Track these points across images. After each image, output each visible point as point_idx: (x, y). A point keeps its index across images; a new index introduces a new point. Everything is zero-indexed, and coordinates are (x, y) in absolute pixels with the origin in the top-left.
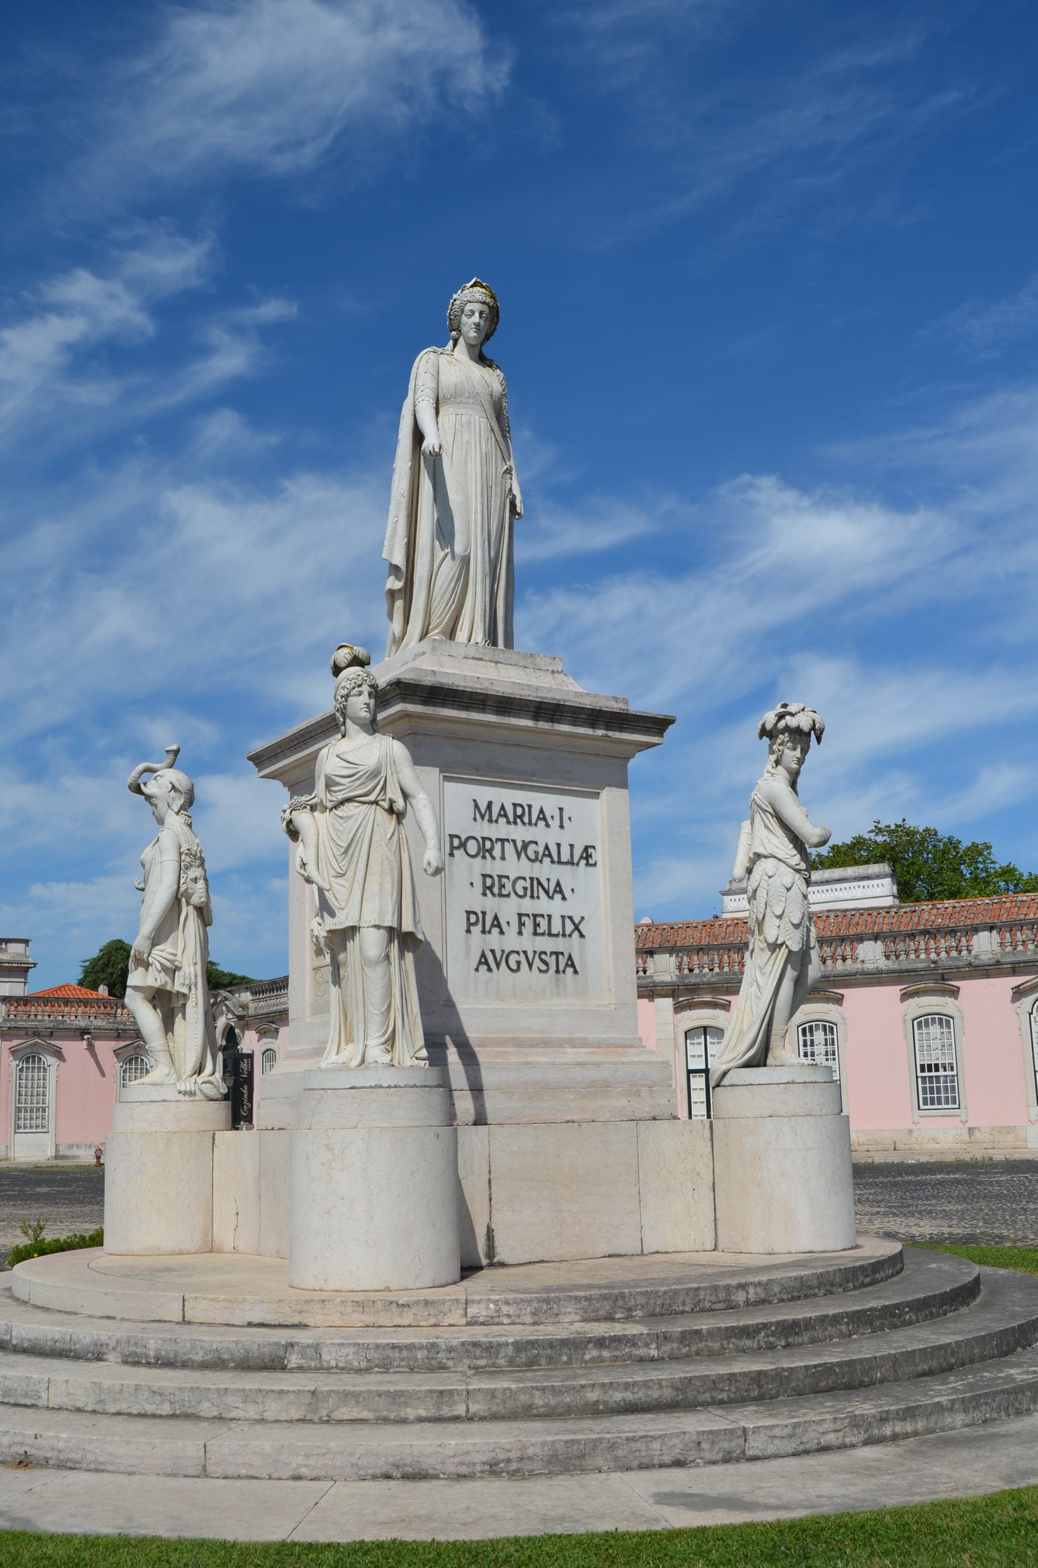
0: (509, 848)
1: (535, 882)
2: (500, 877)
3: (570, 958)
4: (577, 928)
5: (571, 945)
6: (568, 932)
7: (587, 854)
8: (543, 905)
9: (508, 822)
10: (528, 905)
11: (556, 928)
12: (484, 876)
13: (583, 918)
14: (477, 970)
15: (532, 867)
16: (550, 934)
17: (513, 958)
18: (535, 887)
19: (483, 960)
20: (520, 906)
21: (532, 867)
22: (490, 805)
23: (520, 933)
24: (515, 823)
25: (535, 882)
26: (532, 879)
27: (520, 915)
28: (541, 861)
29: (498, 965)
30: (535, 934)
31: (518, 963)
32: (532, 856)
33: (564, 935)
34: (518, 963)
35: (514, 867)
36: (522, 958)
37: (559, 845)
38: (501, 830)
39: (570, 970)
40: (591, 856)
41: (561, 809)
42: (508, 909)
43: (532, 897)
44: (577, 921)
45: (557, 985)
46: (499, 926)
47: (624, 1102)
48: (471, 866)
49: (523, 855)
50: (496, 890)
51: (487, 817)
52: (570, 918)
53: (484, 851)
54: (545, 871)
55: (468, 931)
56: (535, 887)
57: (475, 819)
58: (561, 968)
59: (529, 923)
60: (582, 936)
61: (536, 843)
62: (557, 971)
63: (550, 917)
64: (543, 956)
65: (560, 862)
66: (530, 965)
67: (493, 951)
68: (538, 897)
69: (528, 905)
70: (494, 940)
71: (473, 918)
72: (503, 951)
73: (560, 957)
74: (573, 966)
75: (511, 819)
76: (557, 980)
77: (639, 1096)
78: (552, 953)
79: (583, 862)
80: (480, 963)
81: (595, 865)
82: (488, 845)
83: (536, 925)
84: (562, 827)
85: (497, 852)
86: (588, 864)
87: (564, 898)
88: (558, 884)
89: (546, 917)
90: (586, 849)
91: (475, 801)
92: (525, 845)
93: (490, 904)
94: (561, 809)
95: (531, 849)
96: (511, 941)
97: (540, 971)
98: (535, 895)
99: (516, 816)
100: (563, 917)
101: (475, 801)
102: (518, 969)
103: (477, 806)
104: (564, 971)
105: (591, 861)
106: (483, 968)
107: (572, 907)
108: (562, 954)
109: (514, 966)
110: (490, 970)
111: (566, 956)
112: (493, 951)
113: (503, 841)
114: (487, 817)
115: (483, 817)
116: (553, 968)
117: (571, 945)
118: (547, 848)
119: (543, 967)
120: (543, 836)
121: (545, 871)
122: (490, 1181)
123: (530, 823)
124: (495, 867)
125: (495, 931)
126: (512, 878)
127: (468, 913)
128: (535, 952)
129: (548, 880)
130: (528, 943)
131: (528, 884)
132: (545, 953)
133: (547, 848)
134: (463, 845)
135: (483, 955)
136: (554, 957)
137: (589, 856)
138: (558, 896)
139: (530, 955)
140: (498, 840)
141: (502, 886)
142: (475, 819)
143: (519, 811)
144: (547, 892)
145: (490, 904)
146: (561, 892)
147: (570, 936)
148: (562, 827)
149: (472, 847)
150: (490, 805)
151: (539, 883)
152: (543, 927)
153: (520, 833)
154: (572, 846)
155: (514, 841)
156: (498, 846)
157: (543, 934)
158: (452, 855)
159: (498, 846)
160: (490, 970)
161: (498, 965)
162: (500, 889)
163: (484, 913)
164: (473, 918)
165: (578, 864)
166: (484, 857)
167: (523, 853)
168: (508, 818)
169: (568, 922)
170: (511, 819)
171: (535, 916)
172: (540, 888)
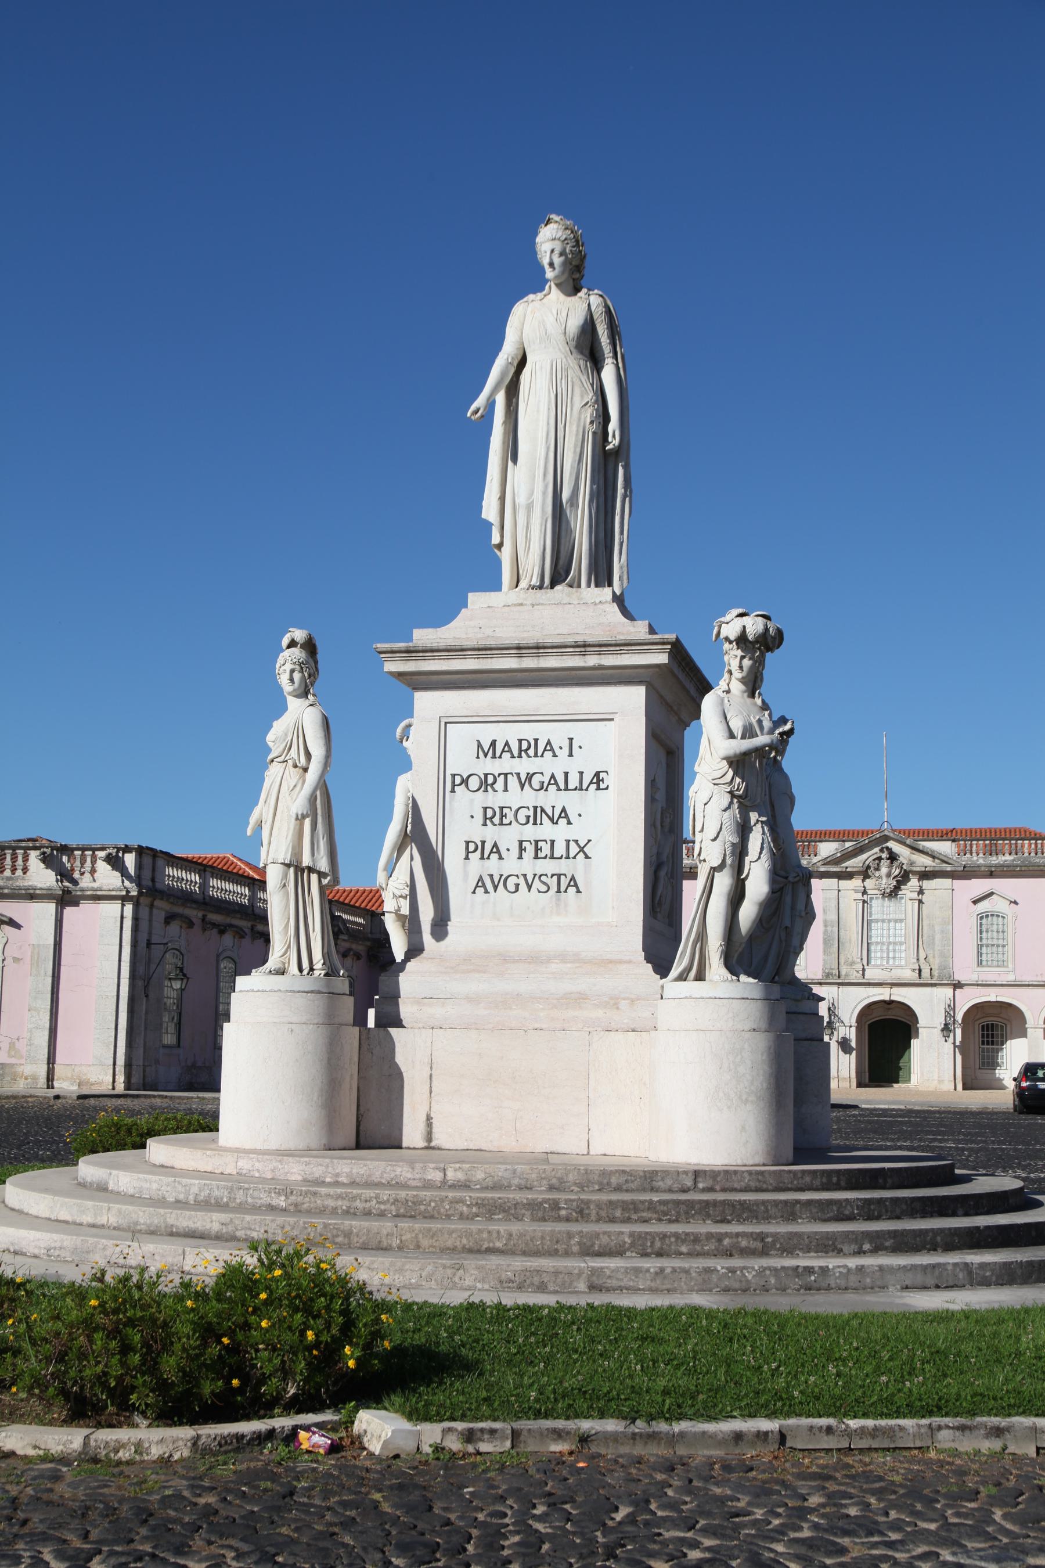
0: (513, 781)
1: (539, 810)
2: (501, 808)
3: (573, 878)
4: (582, 849)
5: (577, 867)
6: (572, 855)
7: (598, 779)
8: (546, 830)
9: (513, 757)
10: (530, 832)
11: (560, 850)
12: (485, 809)
13: (589, 841)
14: (474, 892)
15: (536, 797)
16: (552, 857)
17: (511, 883)
18: (537, 814)
19: (480, 882)
20: (521, 834)
21: (536, 797)
22: (493, 743)
23: (520, 857)
24: (520, 756)
25: (539, 810)
26: (535, 808)
27: (521, 842)
28: (546, 790)
29: (496, 888)
30: (536, 857)
31: (517, 886)
32: (536, 786)
33: (568, 857)
34: (517, 886)
35: (516, 798)
36: (522, 881)
37: (566, 774)
38: (506, 764)
39: (572, 890)
40: (602, 780)
41: (571, 739)
42: (508, 837)
43: (535, 823)
44: (582, 844)
45: (558, 905)
46: (498, 852)
47: (600, 1013)
48: (472, 801)
49: (527, 785)
50: (496, 820)
51: (490, 754)
52: (576, 841)
53: (486, 784)
54: (552, 799)
55: (467, 858)
56: (537, 814)
57: (478, 757)
58: (563, 889)
59: (530, 849)
60: (587, 857)
61: (542, 773)
62: (559, 891)
63: (553, 842)
64: (543, 878)
65: (566, 789)
66: (529, 887)
67: (491, 876)
68: (541, 824)
69: (530, 832)
70: (493, 865)
71: (472, 847)
72: (501, 876)
73: (562, 877)
74: (576, 885)
75: (516, 754)
76: (559, 900)
77: (618, 1008)
78: (552, 876)
79: (594, 786)
80: (477, 886)
81: (607, 788)
82: (490, 779)
83: (537, 849)
84: (571, 755)
85: (500, 785)
86: (598, 788)
87: (569, 823)
88: (564, 810)
89: (549, 843)
90: (597, 774)
91: (478, 741)
92: (530, 777)
93: (491, 834)
94: (571, 739)
95: (536, 781)
96: (511, 865)
97: (539, 892)
98: (538, 822)
99: (520, 750)
100: (568, 841)
101: (478, 741)
102: (517, 890)
103: (480, 745)
104: (566, 891)
105: (602, 786)
106: (480, 890)
107: (578, 831)
108: (565, 875)
109: (512, 888)
110: (486, 892)
111: (569, 877)
112: (491, 876)
113: (506, 775)
114: (490, 754)
115: (486, 755)
116: (554, 888)
117: (577, 867)
118: (553, 776)
119: (544, 888)
120: (547, 766)
121: (552, 799)
122: (431, 1076)
123: (536, 755)
124: (495, 799)
125: (495, 856)
126: (514, 809)
127: (467, 843)
128: (535, 875)
129: (553, 807)
130: (528, 866)
131: (531, 813)
132: (546, 875)
133: (553, 776)
134: (465, 782)
135: (481, 879)
136: (555, 877)
137: (599, 781)
138: (563, 822)
139: (530, 879)
140: (500, 775)
141: (503, 816)
142: (478, 757)
143: (525, 746)
144: (551, 819)
145: (491, 834)
146: (567, 817)
147: (574, 857)
148: (571, 755)
149: (474, 783)
150: (493, 743)
151: (543, 810)
152: (546, 849)
153: (525, 766)
154: (581, 773)
155: (518, 774)
156: (501, 780)
157: (545, 857)
158: (453, 791)
159: (501, 780)
160: (486, 892)
161: (496, 888)
162: (501, 819)
163: (483, 843)
164: (472, 847)
165: (587, 789)
166: (486, 791)
167: (527, 785)
168: (512, 753)
169: (572, 844)
170: (516, 754)
171: (537, 842)
172: (543, 814)
